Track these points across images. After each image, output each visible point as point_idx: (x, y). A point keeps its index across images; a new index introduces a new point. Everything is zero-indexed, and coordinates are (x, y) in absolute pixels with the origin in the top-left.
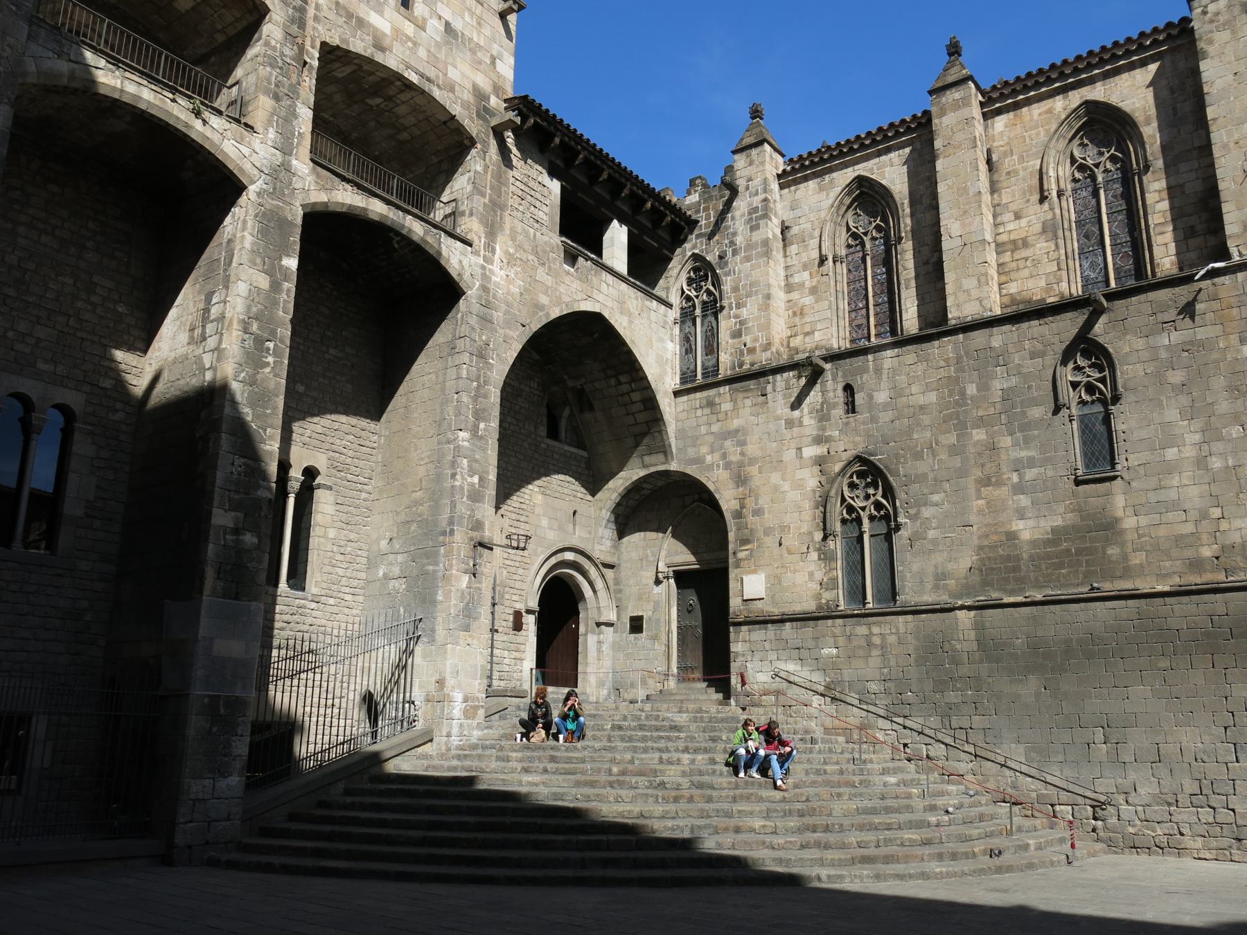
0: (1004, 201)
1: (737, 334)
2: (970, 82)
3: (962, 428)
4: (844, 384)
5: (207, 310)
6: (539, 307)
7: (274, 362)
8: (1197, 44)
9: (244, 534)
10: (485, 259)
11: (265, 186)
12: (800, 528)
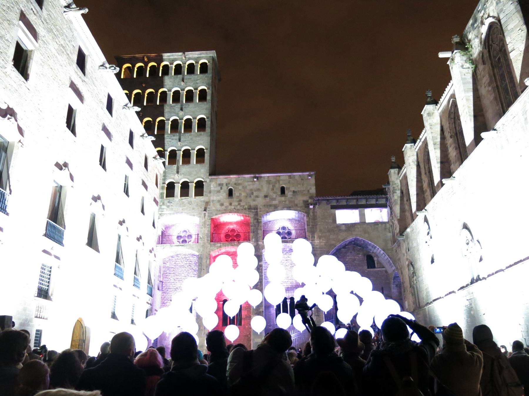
10: (312, 241)
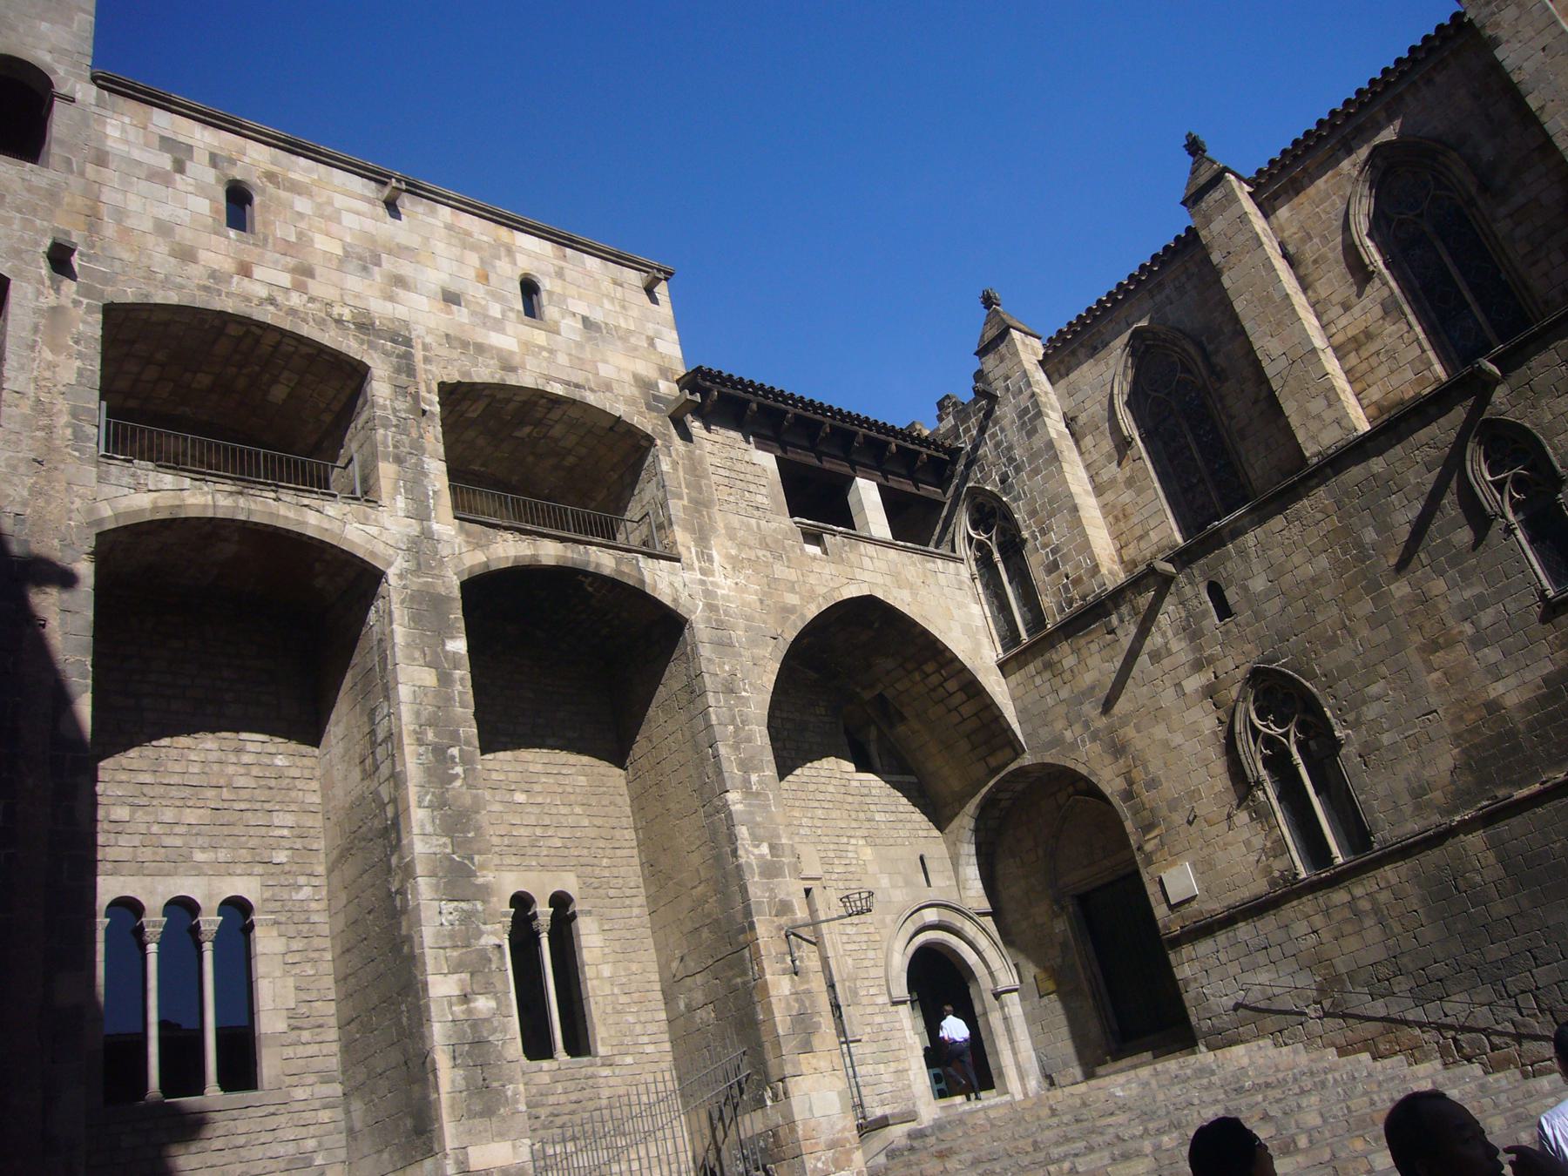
0: (1323, 296)
1: (1052, 567)
2: (1227, 174)
4: (1206, 583)
5: (373, 732)
6: (787, 610)
7: (464, 771)
8: (1482, 33)
9: (476, 1000)
10: (703, 572)
11: (405, 565)
12: (1213, 787)
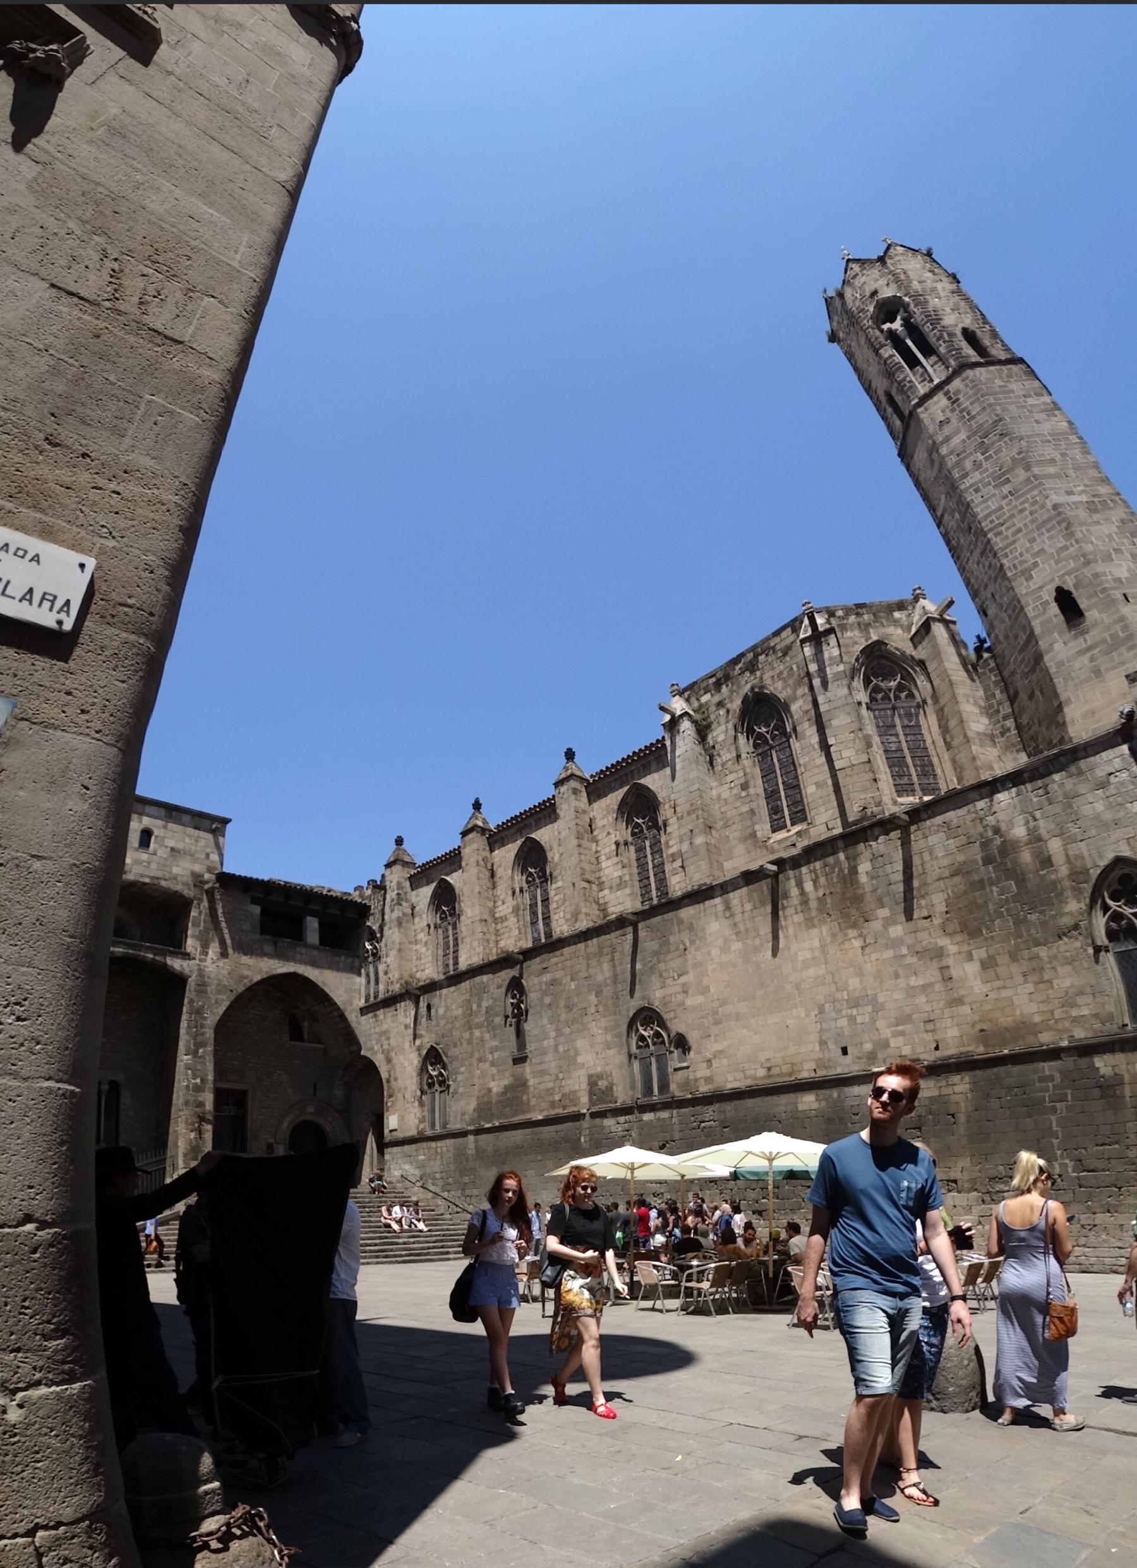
3: (470, 1028)
